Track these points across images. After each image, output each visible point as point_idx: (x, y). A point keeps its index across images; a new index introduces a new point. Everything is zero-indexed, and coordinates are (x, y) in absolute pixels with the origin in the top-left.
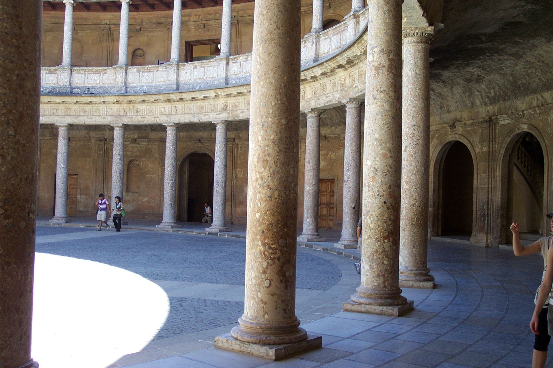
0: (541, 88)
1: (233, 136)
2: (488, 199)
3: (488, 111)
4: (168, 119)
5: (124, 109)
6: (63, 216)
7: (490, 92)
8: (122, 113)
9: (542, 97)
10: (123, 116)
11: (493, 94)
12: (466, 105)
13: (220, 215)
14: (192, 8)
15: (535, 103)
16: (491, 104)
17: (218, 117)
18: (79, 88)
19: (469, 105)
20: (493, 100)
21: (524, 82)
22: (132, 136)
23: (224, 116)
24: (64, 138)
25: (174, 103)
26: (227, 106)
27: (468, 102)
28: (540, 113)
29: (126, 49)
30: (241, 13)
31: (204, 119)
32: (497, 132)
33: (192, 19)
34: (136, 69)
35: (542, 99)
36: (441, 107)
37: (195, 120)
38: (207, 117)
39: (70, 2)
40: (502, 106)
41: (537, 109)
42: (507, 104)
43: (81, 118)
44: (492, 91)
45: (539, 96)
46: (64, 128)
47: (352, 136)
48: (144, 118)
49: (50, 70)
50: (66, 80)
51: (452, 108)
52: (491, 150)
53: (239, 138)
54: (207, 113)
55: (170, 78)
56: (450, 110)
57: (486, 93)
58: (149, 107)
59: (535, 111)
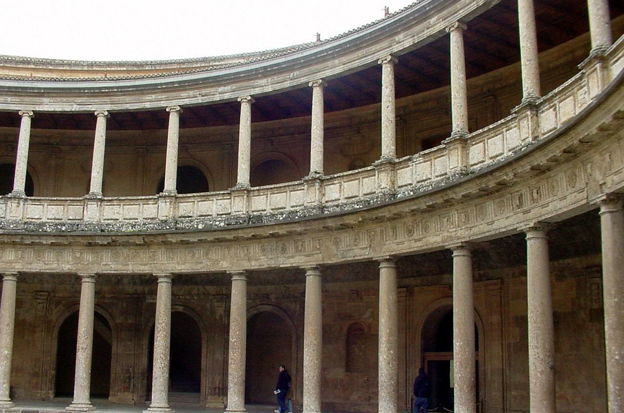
16: (141, 284)
45: (201, 288)
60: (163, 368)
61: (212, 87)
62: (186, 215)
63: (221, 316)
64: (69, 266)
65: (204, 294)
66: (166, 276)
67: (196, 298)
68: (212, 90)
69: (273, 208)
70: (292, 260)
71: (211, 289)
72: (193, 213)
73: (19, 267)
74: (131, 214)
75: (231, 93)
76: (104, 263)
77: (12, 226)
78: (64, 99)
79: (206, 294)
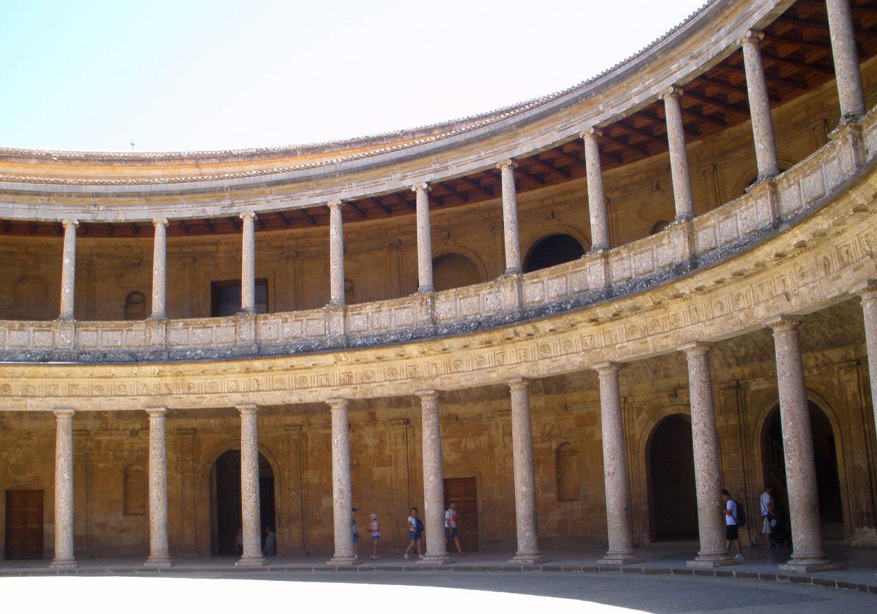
1: (299, 422)
2: (745, 484)
3: (733, 374)
4: (245, 399)
5: (166, 385)
6: (70, 557)
7: (739, 351)
8: (164, 390)
9: (824, 355)
10: (166, 395)
13: (349, 540)
14: (222, 233)
16: (738, 365)
17: (335, 394)
18: (89, 353)
22: (130, 427)
23: (346, 392)
24: (67, 433)
25: (255, 374)
26: (351, 377)
29: (164, 294)
30: (300, 241)
31: (309, 397)
32: (748, 399)
33: (221, 248)
34: (182, 323)
35: (822, 358)
36: (655, 372)
37: (294, 399)
38: (314, 394)
39: (73, 224)
43: (95, 400)
45: (819, 355)
46: (67, 416)
47: (615, 412)
48: (204, 397)
49: (40, 326)
50: (68, 342)
52: (742, 422)
53: (310, 424)
54: (314, 389)
55: (244, 337)
57: (733, 352)
58: (210, 381)
60: (707, 493)
61: (703, 38)
62: (708, 248)
63: (854, 394)
64: (579, 359)
65: (825, 365)
66: (693, 349)
67: (815, 372)
68: (703, 46)
69: (809, 200)
70: (839, 283)
71: (835, 354)
72: (716, 241)
73: (523, 370)
74: (644, 264)
75: (726, 38)
76: (618, 346)
77: (507, 318)
78: (542, 129)
79: (828, 364)
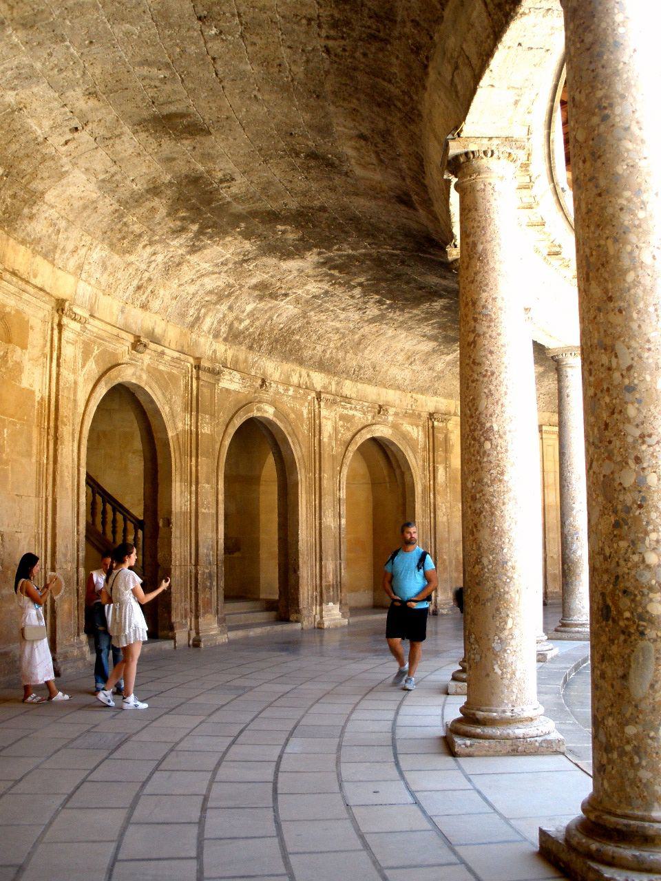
0: (314, 362)
7: (241, 321)
9: (308, 375)
11: (242, 327)
12: (183, 315)
15: (295, 379)
16: (225, 340)
19: (190, 319)
20: (234, 337)
21: (302, 340)
27: (192, 311)
28: (294, 398)
40: (242, 356)
41: (292, 389)
42: (252, 357)
44: (247, 322)
45: (304, 372)
51: (155, 304)
56: (151, 305)
59: (287, 390)
